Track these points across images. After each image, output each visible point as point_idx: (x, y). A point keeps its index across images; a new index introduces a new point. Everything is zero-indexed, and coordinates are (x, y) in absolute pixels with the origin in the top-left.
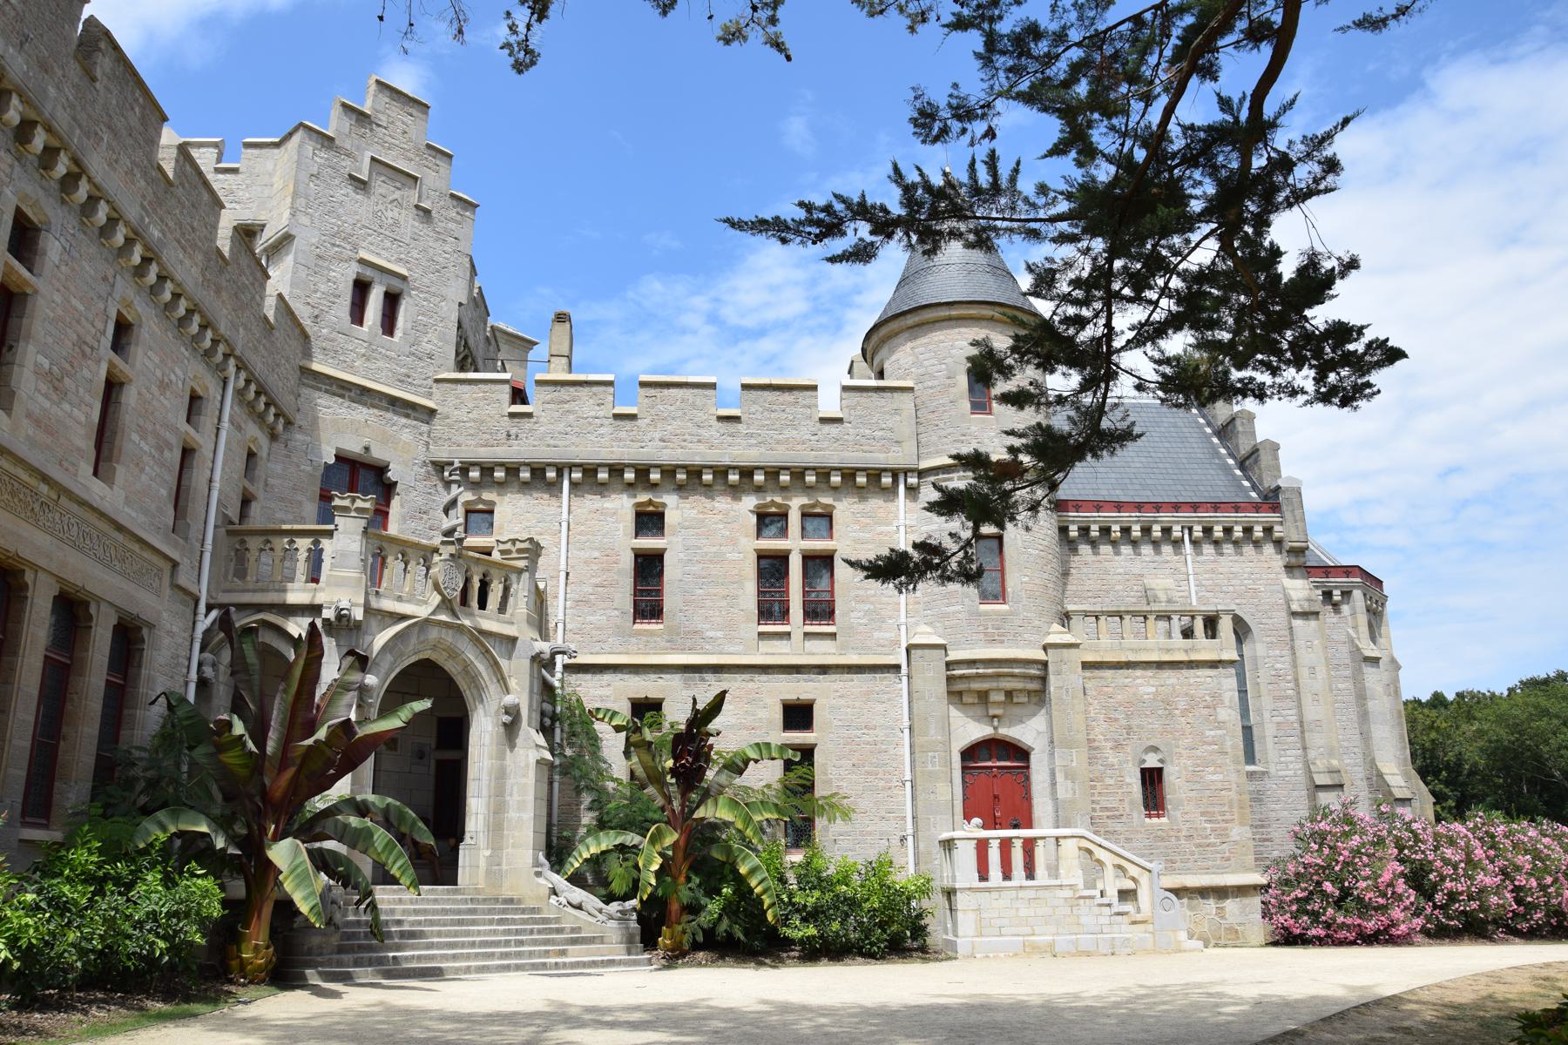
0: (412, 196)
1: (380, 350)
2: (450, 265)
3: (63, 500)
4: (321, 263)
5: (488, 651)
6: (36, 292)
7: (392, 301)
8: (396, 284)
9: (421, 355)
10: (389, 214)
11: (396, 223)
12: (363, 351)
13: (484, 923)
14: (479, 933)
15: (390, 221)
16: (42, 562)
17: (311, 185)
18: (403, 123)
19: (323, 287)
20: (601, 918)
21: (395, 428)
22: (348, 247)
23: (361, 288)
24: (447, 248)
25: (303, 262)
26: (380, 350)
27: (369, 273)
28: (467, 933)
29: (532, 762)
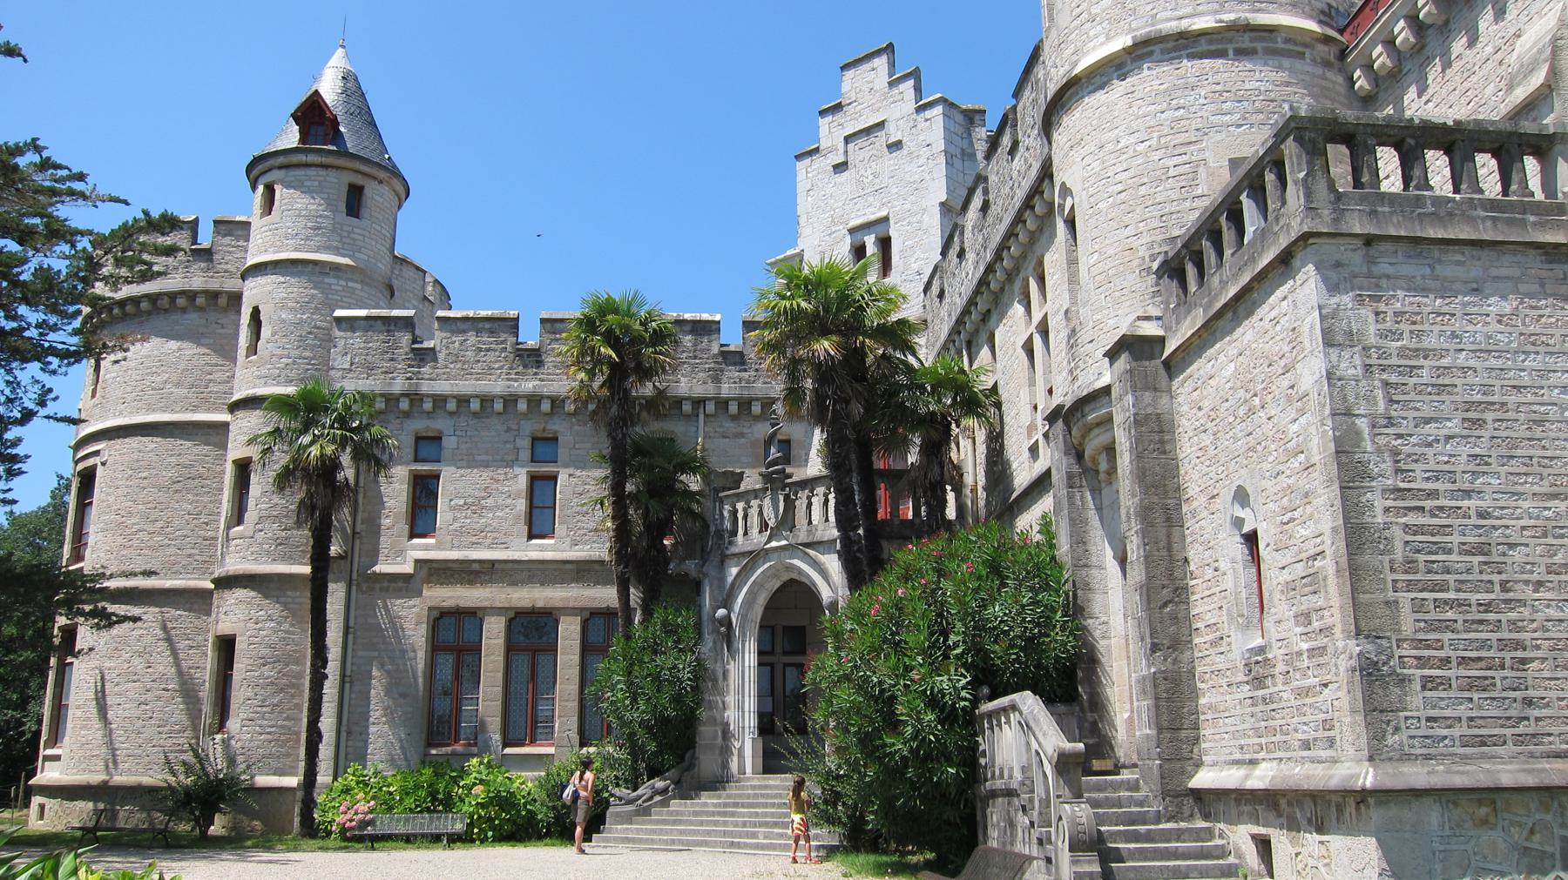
0: (880, 139)
7: (885, 244)
9: (911, 278)
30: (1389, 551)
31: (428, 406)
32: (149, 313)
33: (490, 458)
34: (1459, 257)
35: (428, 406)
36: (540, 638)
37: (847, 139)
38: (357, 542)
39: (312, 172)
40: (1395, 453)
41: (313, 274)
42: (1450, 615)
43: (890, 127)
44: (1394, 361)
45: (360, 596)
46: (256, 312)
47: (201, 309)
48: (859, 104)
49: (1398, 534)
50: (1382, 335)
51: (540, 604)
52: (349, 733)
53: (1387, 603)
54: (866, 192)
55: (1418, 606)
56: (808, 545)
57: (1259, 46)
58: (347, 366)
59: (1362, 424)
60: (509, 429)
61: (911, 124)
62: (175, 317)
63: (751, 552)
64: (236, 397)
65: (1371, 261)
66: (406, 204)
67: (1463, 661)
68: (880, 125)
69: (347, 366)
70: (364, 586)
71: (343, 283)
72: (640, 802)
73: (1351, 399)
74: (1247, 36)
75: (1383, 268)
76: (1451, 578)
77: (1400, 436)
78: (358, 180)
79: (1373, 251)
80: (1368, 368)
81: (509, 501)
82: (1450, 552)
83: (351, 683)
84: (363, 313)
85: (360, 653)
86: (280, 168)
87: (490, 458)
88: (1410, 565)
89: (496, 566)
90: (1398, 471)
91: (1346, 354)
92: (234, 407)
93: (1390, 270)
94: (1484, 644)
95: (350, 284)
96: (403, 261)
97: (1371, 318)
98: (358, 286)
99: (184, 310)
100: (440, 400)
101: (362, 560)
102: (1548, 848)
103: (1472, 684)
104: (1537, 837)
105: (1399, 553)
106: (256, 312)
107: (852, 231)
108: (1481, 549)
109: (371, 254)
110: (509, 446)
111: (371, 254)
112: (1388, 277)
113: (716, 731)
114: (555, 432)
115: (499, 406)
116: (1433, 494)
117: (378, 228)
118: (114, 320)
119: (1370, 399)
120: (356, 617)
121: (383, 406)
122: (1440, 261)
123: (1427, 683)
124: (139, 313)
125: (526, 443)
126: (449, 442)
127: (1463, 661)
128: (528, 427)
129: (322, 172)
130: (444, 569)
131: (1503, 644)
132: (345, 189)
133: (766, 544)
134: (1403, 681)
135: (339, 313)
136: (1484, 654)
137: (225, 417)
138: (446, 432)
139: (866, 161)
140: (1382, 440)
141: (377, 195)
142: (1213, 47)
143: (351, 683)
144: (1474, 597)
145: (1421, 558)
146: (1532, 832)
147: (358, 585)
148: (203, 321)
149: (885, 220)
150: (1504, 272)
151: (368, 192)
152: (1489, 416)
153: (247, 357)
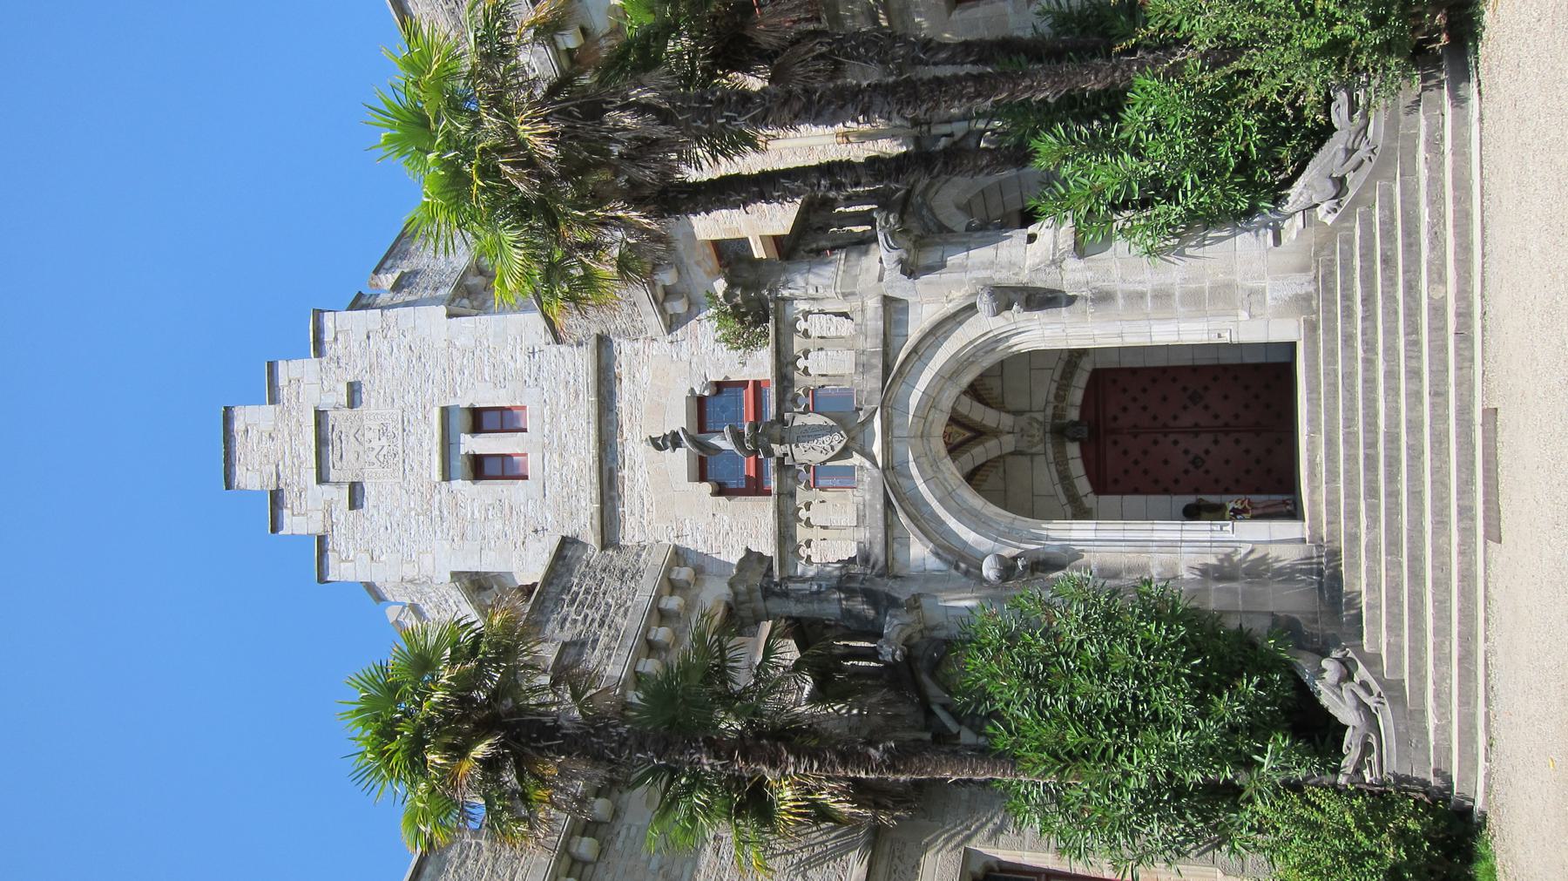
0: (339, 419)
1: (546, 431)
2: (405, 341)
4: (469, 533)
5: (915, 350)
7: (478, 420)
8: (460, 421)
9: (535, 369)
10: (376, 444)
11: (383, 431)
12: (555, 456)
13: (1370, 403)
14: (1393, 412)
15: (384, 439)
17: (383, 558)
18: (260, 441)
19: (498, 526)
20: (1363, 151)
21: (640, 396)
22: (437, 498)
23: (479, 468)
24: (385, 348)
25: (477, 557)
26: (546, 431)
27: (459, 464)
28: (1393, 439)
29: (1080, 264)
37: (322, 479)
43: (327, 402)
48: (283, 457)
54: (400, 452)
56: (887, 369)
61: (333, 366)
63: (888, 503)
68: (320, 416)
72: (1370, 701)
107: (447, 476)
113: (1218, 590)
133: (875, 464)
139: (360, 449)
149: (445, 412)
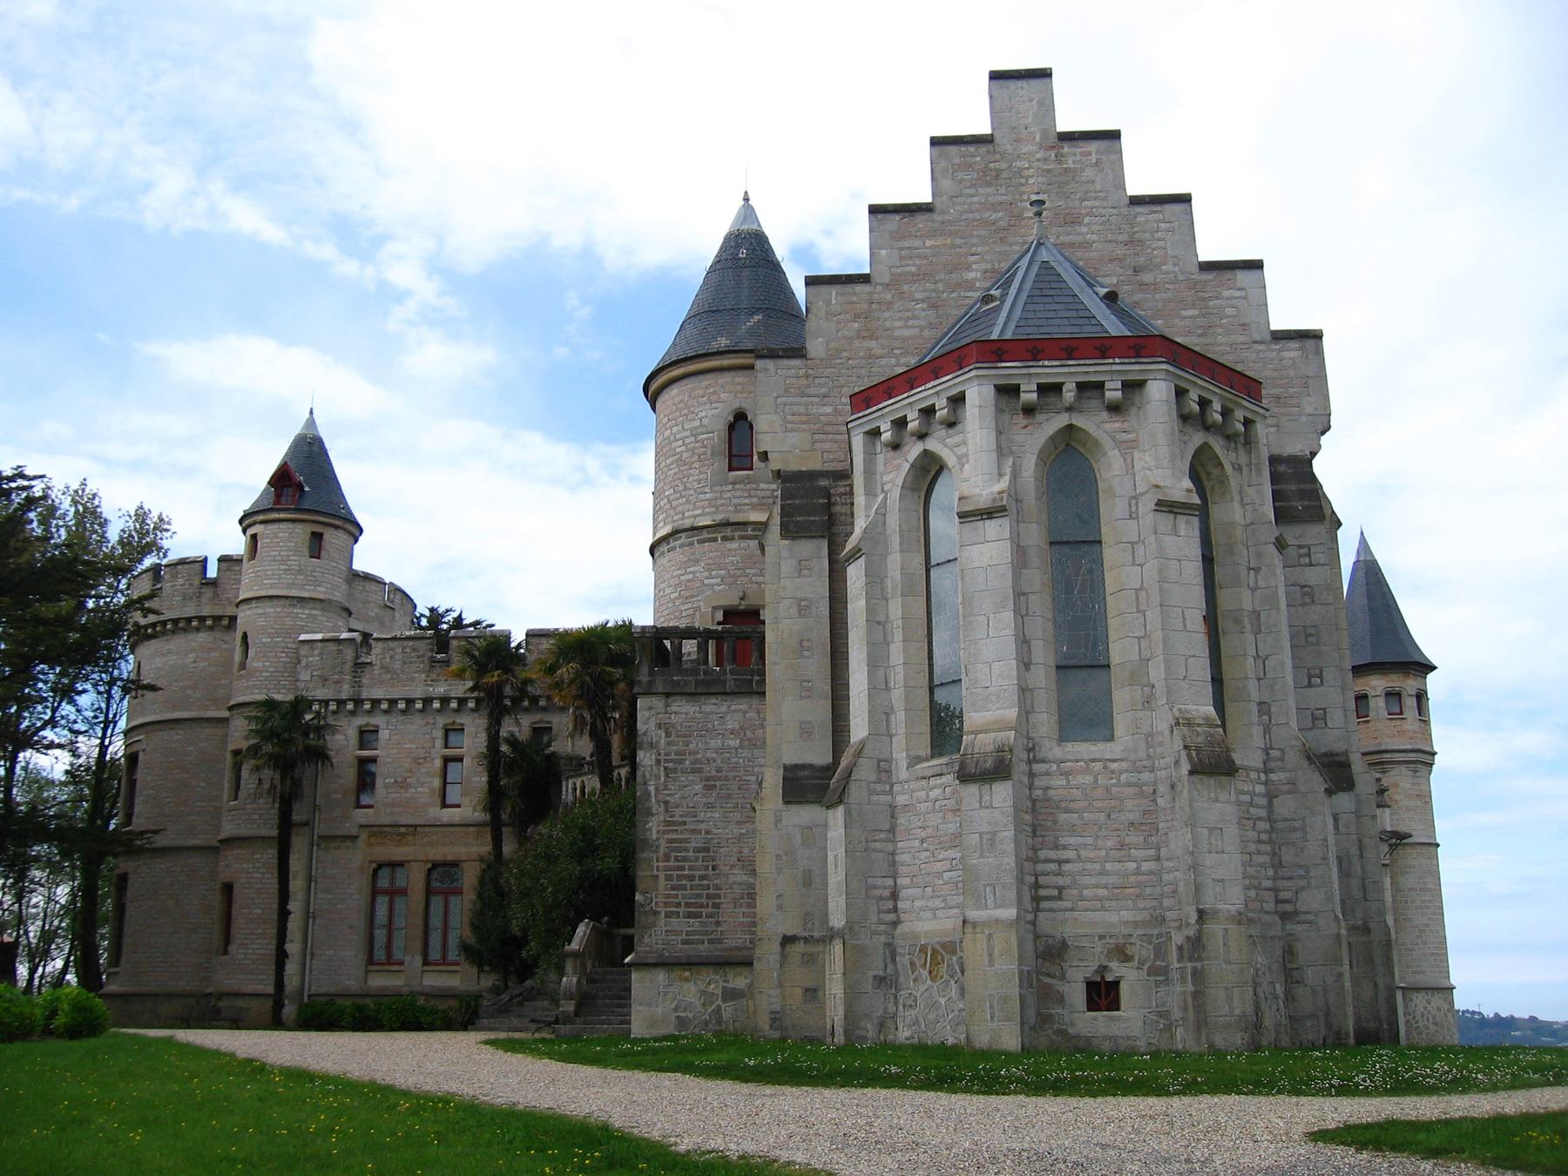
3: (418, 829)
6: (377, 756)
16: (409, 858)
30: (656, 851)
31: (367, 706)
32: (173, 632)
33: (414, 746)
34: (714, 701)
35: (367, 706)
36: (452, 883)
38: (317, 813)
39: (283, 526)
40: (666, 803)
41: (285, 606)
42: (684, 882)
44: (673, 757)
45: (320, 852)
46: (245, 636)
47: (211, 628)
49: (663, 843)
50: (669, 744)
51: (450, 858)
52: (312, 954)
53: (653, 876)
55: (668, 878)
57: (737, 534)
58: (308, 678)
59: (652, 789)
60: (427, 724)
62: (190, 636)
64: (232, 703)
65: (667, 705)
66: (361, 538)
67: (688, 905)
69: (308, 678)
70: (323, 845)
71: (307, 612)
73: (648, 775)
74: (729, 529)
75: (674, 708)
76: (687, 864)
77: (669, 795)
78: (318, 529)
79: (670, 701)
80: (658, 762)
81: (427, 780)
82: (688, 851)
83: (314, 917)
84: (319, 636)
85: (320, 896)
86: (262, 522)
87: (414, 746)
88: (667, 858)
89: (418, 829)
90: (667, 811)
91: (648, 755)
92: (230, 709)
93: (677, 709)
94: (698, 896)
95: (314, 612)
96: (368, 578)
97: (663, 735)
98: (320, 613)
99: (198, 629)
100: (376, 702)
101: (322, 825)
102: (715, 992)
103: (690, 915)
104: (712, 986)
105: (662, 850)
106: (245, 636)
108: (707, 850)
109: (329, 586)
110: (427, 736)
111: (329, 586)
112: (676, 713)
114: (462, 725)
115: (419, 705)
116: (684, 823)
117: (334, 564)
118: (149, 637)
119: (658, 777)
120: (317, 869)
121: (335, 707)
122: (705, 704)
123: (668, 915)
124: (164, 633)
125: (439, 734)
126: (384, 735)
127: (688, 905)
128: (442, 721)
129: (291, 525)
130: (381, 832)
131: (708, 896)
132: (309, 536)
134: (656, 913)
135: (303, 637)
136: (698, 901)
137: (226, 714)
138: (381, 727)
140: (660, 797)
141: (332, 538)
142: (710, 536)
143: (314, 917)
144: (697, 873)
145: (673, 854)
146: (709, 983)
147: (318, 845)
148: (211, 639)
150: (739, 707)
151: (326, 537)
152: (718, 783)
153: (239, 671)
